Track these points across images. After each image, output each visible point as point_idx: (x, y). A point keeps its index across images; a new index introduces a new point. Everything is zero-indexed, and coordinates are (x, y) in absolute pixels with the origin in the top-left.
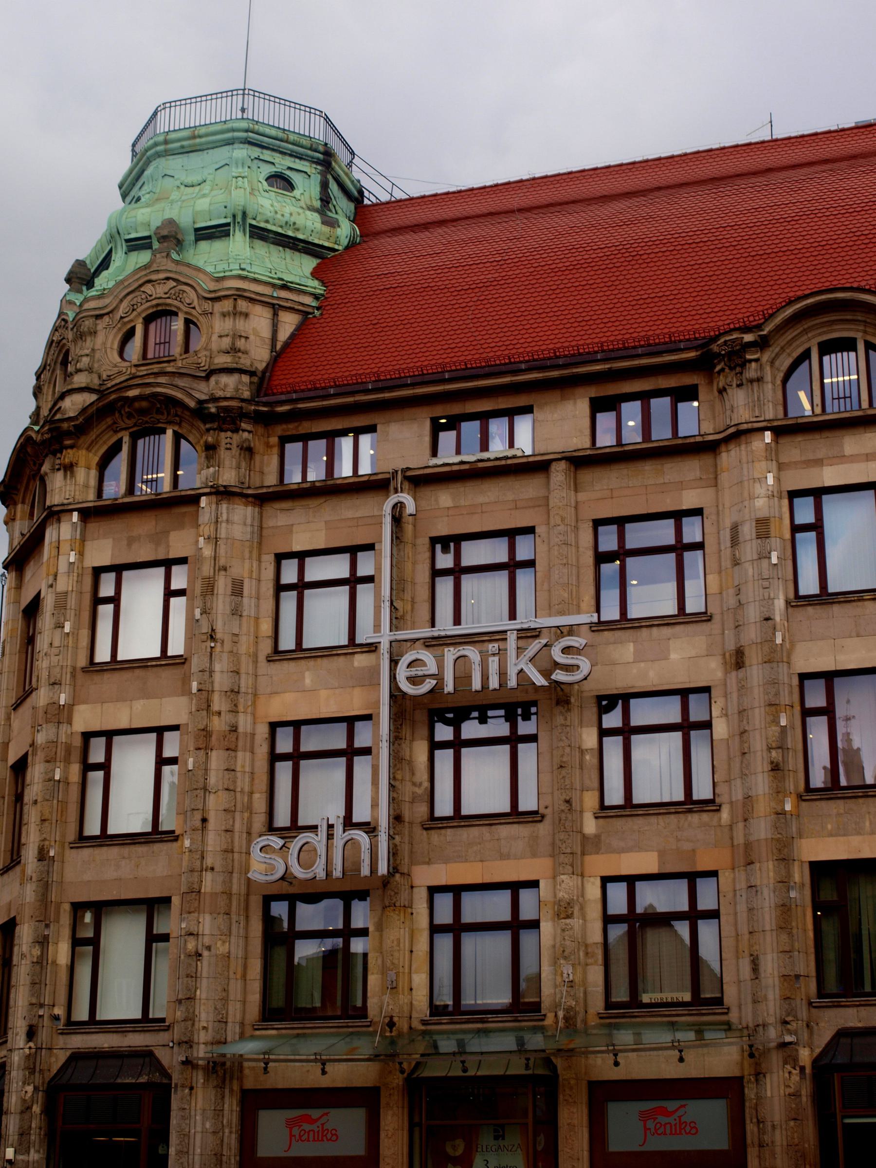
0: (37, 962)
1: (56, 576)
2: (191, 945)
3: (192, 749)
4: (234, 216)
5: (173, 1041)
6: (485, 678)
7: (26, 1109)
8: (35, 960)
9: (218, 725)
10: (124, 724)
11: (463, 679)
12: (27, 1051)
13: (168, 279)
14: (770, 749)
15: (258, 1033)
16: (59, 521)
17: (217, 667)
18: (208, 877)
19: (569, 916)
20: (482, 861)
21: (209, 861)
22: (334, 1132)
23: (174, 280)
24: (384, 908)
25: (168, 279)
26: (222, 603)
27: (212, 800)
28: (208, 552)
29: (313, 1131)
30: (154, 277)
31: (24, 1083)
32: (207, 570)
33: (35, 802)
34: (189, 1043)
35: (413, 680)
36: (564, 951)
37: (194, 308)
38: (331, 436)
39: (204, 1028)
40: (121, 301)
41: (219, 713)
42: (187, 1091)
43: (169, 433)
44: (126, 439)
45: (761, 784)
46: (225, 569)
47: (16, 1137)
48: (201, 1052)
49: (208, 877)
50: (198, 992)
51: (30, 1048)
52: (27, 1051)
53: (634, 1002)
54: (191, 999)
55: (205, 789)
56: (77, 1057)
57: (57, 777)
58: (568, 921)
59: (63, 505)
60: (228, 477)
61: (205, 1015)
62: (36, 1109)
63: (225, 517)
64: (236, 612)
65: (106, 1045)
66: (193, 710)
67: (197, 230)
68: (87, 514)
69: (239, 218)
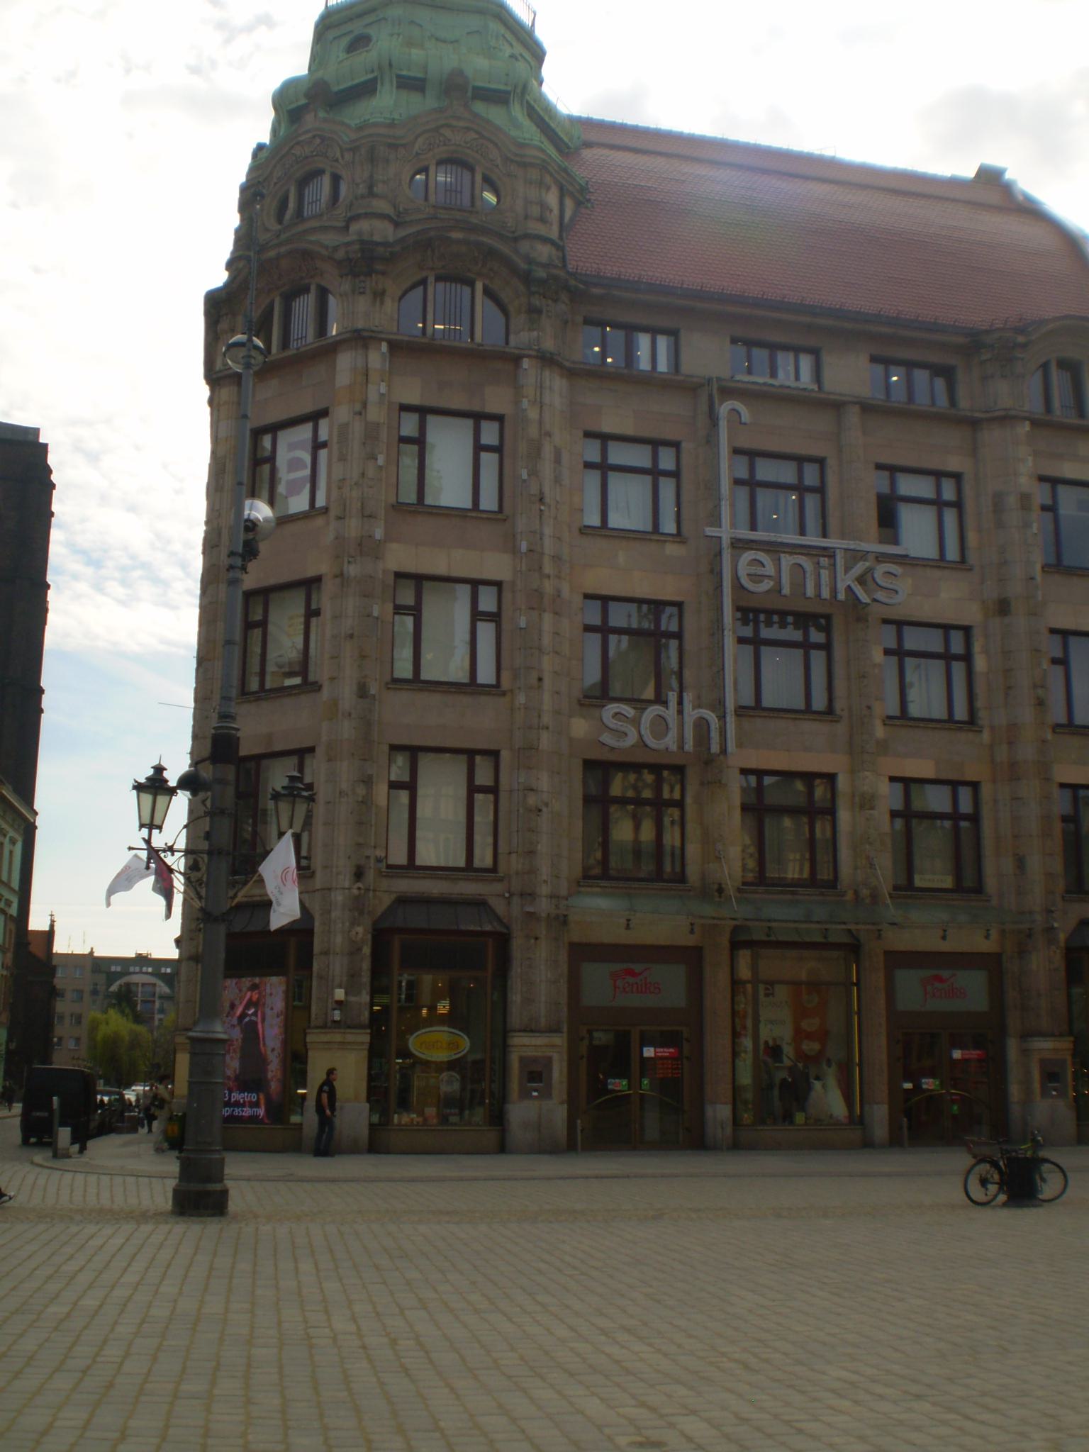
0: (362, 802)
1: (365, 405)
2: (532, 800)
3: (523, 607)
4: (516, 87)
5: (509, 892)
6: (818, 586)
7: (355, 950)
8: (360, 799)
9: (548, 587)
10: (442, 570)
11: (799, 586)
12: (355, 892)
13: (468, 129)
14: (1035, 686)
15: (583, 889)
16: (366, 347)
17: (548, 531)
18: (545, 736)
19: (872, 808)
20: (788, 750)
21: (546, 719)
22: (656, 985)
23: (477, 133)
24: (702, 784)
25: (468, 129)
26: (547, 468)
27: (546, 659)
28: (533, 414)
29: (637, 983)
30: (454, 123)
31: (354, 923)
32: (533, 432)
33: (351, 636)
34: (528, 895)
35: (757, 578)
36: (869, 838)
37: (497, 166)
38: (631, 329)
39: (545, 882)
40: (416, 138)
41: (549, 577)
42: (533, 941)
43: (479, 286)
44: (431, 280)
45: (1026, 715)
46: (550, 436)
47: (345, 979)
48: (544, 906)
49: (545, 736)
50: (539, 847)
51: (359, 888)
52: (355, 892)
53: (910, 885)
54: (532, 853)
55: (540, 649)
56: (403, 901)
57: (375, 614)
58: (871, 812)
59: (373, 331)
60: (549, 345)
61: (545, 871)
62: (367, 950)
63: (548, 383)
64: (557, 480)
65: (435, 891)
66: (524, 568)
67: (475, 88)
68: (395, 347)
69: (519, 90)
